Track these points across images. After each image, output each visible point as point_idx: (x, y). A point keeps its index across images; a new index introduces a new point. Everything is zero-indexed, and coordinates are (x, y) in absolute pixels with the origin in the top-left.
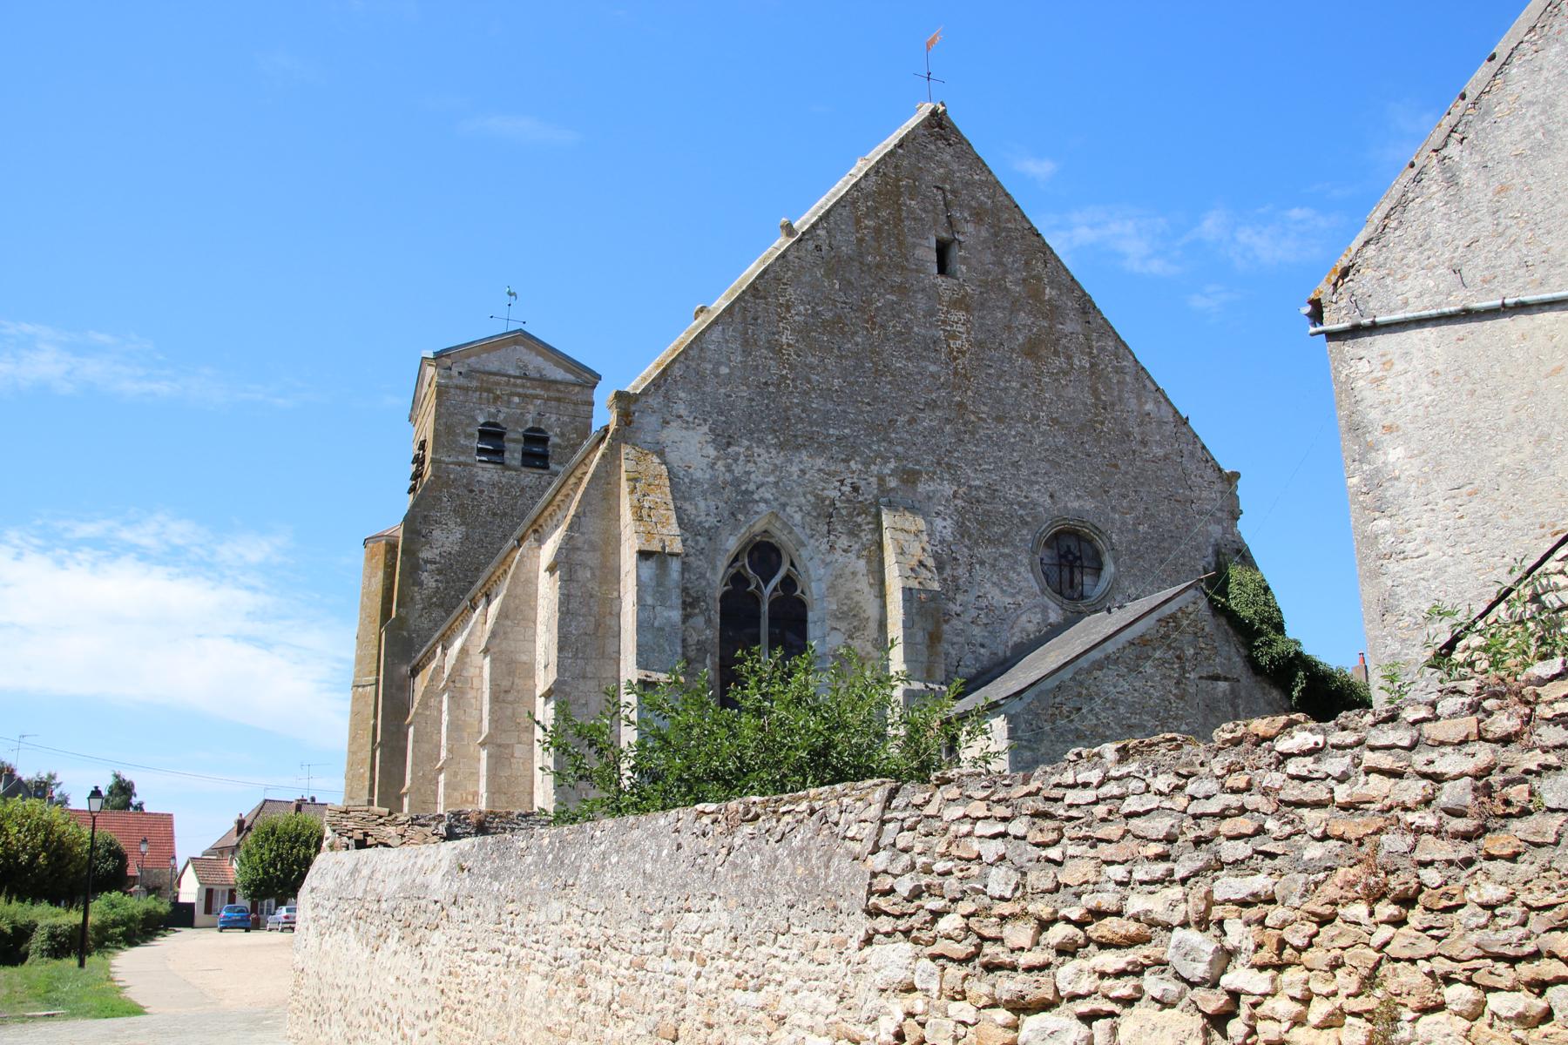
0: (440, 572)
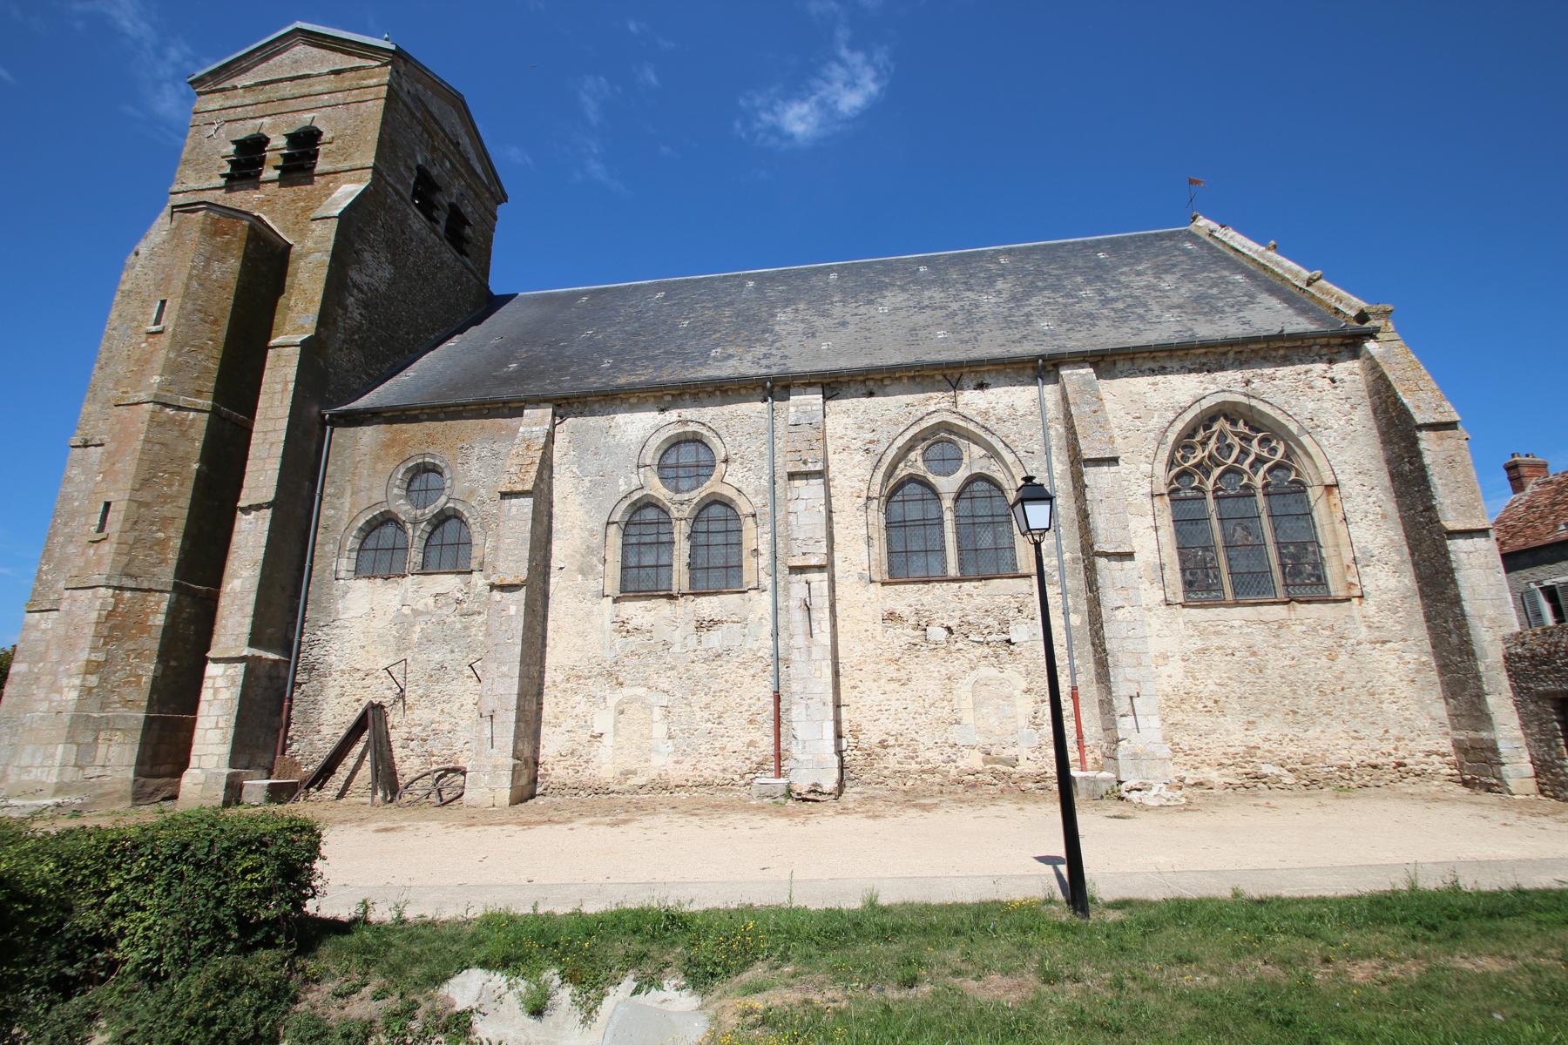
0: (365, 305)
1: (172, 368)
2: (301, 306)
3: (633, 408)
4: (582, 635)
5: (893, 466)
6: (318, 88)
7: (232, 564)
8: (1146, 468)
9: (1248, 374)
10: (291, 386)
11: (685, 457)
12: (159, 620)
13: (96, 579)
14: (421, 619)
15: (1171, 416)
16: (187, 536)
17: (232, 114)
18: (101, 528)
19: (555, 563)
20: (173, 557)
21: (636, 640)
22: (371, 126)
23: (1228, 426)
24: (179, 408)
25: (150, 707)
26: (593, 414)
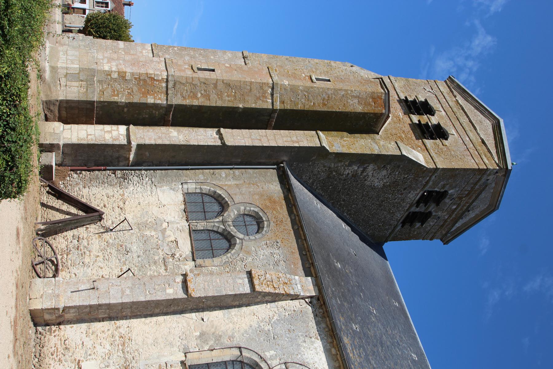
0: (355, 175)
1: (293, 89)
2: (344, 143)
3: (327, 351)
4: (155, 342)
6: (471, 135)
7: (186, 131)
12: (150, 100)
13: (171, 71)
14: (160, 234)
16: (200, 107)
17: (441, 97)
18: (199, 69)
19: (206, 315)
20: (187, 102)
22: (460, 163)
24: (272, 95)
25: (100, 102)
26: (317, 323)
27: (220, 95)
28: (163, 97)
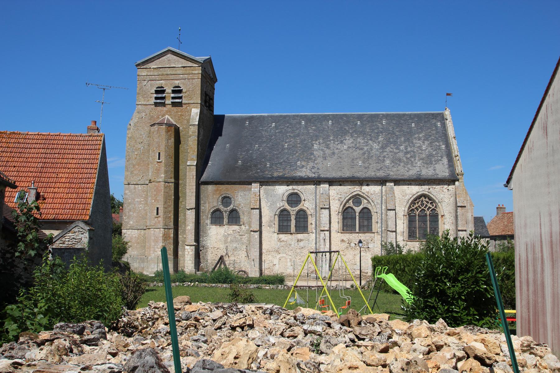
1: (166, 172)
2: (191, 152)
3: (280, 185)
4: (270, 241)
5: (345, 204)
6: (178, 72)
8: (403, 209)
9: (430, 187)
10: (195, 177)
11: (294, 199)
12: (172, 235)
13: (159, 226)
15: (411, 196)
18: (157, 214)
20: (172, 220)
21: (283, 243)
22: (197, 88)
23: (424, 199)
24: (168, 183)
26: (270, 185)
27: (169, 206)
28: (171, 230)
